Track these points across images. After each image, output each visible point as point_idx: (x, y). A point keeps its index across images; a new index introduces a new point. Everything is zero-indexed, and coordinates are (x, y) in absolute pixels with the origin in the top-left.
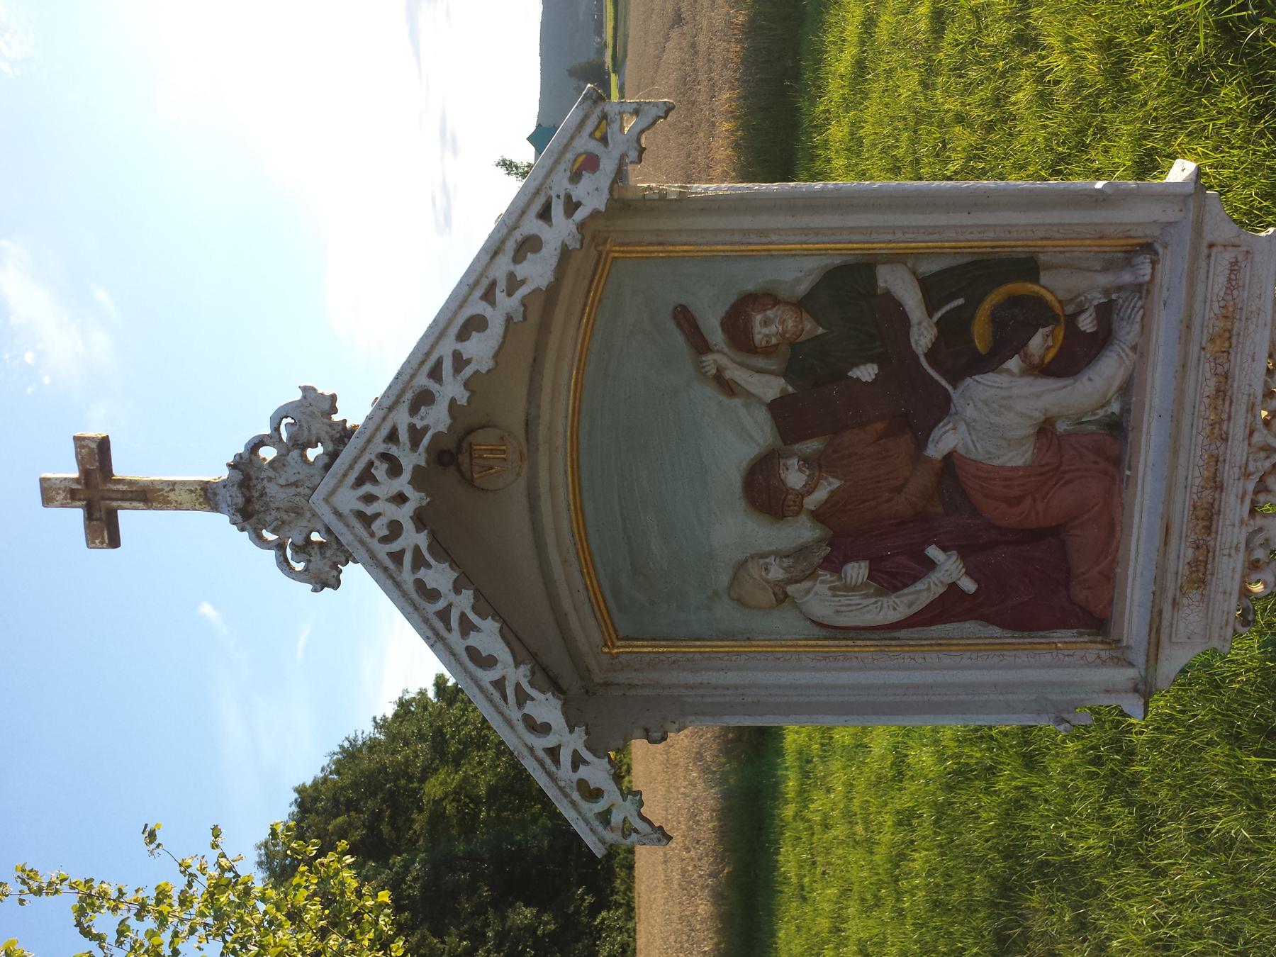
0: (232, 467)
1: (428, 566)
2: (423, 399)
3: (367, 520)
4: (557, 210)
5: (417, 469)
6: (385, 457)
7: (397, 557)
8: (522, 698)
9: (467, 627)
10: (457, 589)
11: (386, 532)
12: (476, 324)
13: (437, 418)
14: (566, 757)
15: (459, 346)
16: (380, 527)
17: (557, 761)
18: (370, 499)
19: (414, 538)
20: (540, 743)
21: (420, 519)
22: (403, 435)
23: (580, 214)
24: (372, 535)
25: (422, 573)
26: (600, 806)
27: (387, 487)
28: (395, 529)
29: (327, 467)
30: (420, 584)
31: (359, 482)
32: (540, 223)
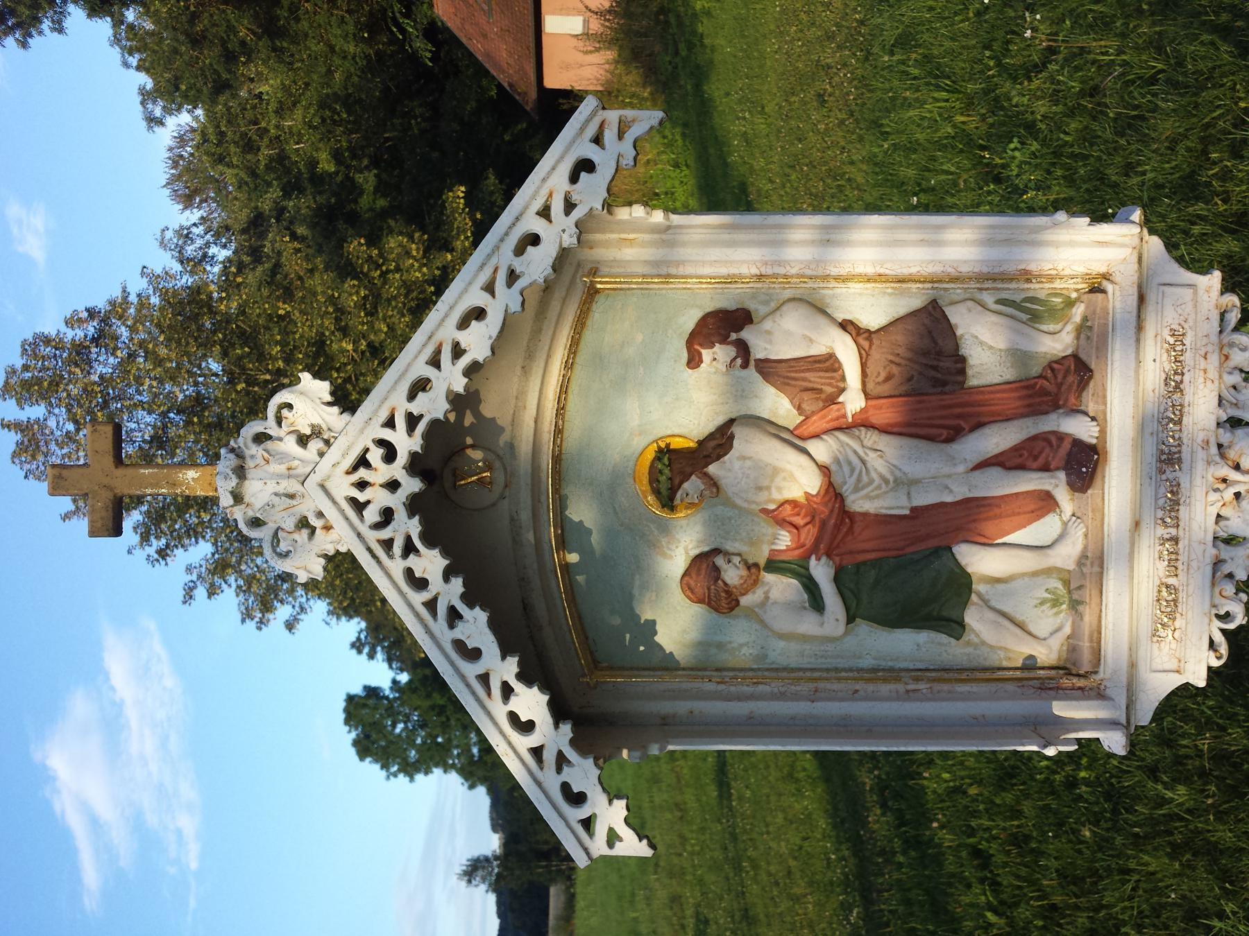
1: (417, 551)
3: (359, 507)
4: (557, 207)
5: (414, 456)
6: (381, 443)
7: (388, 544)
9: (454, 616)
10: (447, 575)
11: (377, 519)
14: (549, 756)
16: (372, 515)
18: (362, 485)
20: (525, 743)
21: (414, 505)
23: (577, 214)
25: (412, 561)
26: (584, 812)
27: (381, 472)
28: (387, 515)
30: (409, 573)
31: (355, 468)
32: (543, 221)
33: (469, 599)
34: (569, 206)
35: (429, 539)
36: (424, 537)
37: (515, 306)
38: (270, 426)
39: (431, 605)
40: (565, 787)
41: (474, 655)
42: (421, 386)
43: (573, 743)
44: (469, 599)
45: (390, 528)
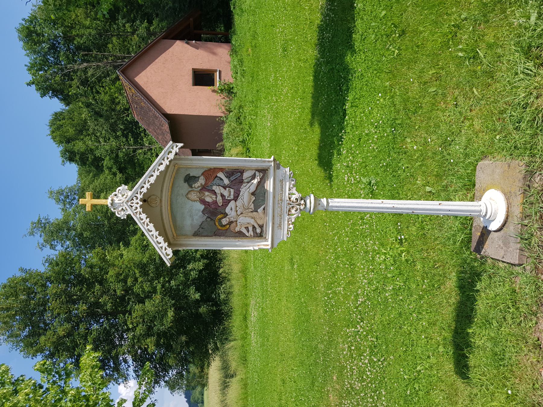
3: (132, 206)
7: (136, 213)
8: (156, 237)
9: (147, 225)
13: (144, 190)
14: (164, 248)
17: (162, 249)
19: (139, 210)
21: (141, 207)
22: (139, 193)
28: (137, 208)
33: (150, 222)
34: (168, 158)
35: (143, 212)
36: (142, 212)
38: (117, 193)
39: (144, 223)
40: (166, 253)
41: (151, 231)
42: (143, 187)
43: (168, 246)
44: (150, 222)
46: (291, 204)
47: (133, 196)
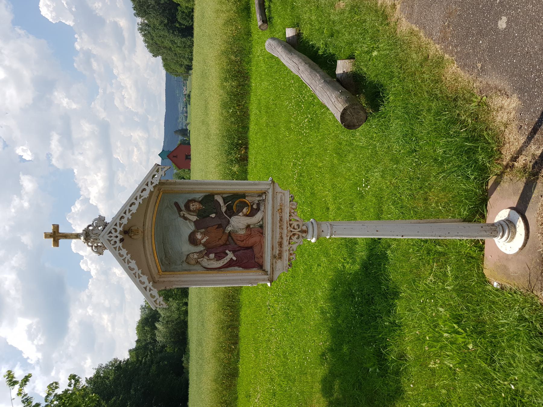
0: (84, 230)
2: (122, 217)
4: (149, 184)
6: (114, 228)
8: (139, 277)
9: (129, 262)
11: (113, 243)
12: (133, 204)
13: (125, 221)
14: (148, 288)
15: (130, 208)
16: (112, 242)
18: (111, 237)
19: (119, 244)
22: (118, 225)
24: (111, 244)
25: (120, 251)
27: (114, 234)
28: (116, 242)
29: (103, 231)
32: (147, 186)
33: (132, 258)
34: (152, 183)
36: (122, 246)
37: (141, 203)
40: (151, 294)
44: (132, 258)
45: (116, 245)
46: (291, 231)
47: (111, 228)
